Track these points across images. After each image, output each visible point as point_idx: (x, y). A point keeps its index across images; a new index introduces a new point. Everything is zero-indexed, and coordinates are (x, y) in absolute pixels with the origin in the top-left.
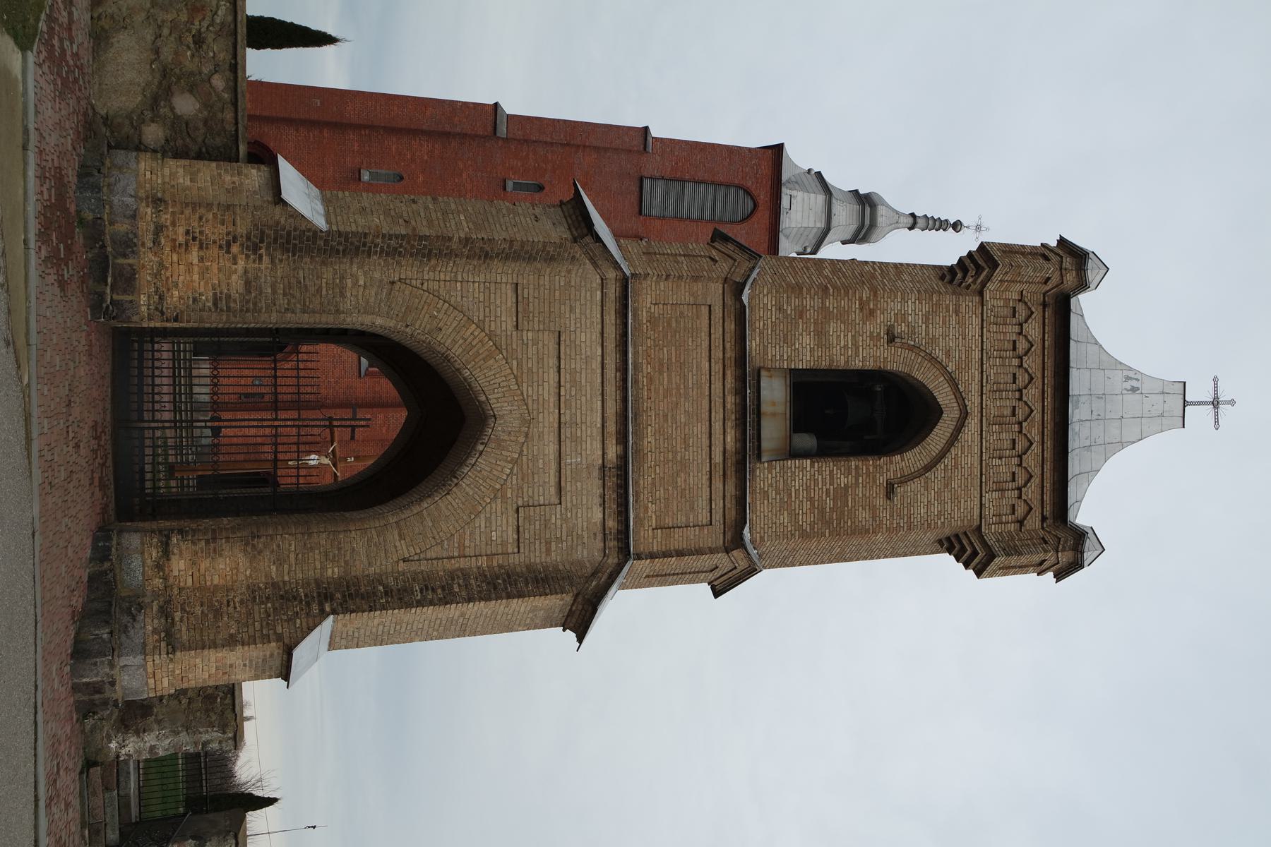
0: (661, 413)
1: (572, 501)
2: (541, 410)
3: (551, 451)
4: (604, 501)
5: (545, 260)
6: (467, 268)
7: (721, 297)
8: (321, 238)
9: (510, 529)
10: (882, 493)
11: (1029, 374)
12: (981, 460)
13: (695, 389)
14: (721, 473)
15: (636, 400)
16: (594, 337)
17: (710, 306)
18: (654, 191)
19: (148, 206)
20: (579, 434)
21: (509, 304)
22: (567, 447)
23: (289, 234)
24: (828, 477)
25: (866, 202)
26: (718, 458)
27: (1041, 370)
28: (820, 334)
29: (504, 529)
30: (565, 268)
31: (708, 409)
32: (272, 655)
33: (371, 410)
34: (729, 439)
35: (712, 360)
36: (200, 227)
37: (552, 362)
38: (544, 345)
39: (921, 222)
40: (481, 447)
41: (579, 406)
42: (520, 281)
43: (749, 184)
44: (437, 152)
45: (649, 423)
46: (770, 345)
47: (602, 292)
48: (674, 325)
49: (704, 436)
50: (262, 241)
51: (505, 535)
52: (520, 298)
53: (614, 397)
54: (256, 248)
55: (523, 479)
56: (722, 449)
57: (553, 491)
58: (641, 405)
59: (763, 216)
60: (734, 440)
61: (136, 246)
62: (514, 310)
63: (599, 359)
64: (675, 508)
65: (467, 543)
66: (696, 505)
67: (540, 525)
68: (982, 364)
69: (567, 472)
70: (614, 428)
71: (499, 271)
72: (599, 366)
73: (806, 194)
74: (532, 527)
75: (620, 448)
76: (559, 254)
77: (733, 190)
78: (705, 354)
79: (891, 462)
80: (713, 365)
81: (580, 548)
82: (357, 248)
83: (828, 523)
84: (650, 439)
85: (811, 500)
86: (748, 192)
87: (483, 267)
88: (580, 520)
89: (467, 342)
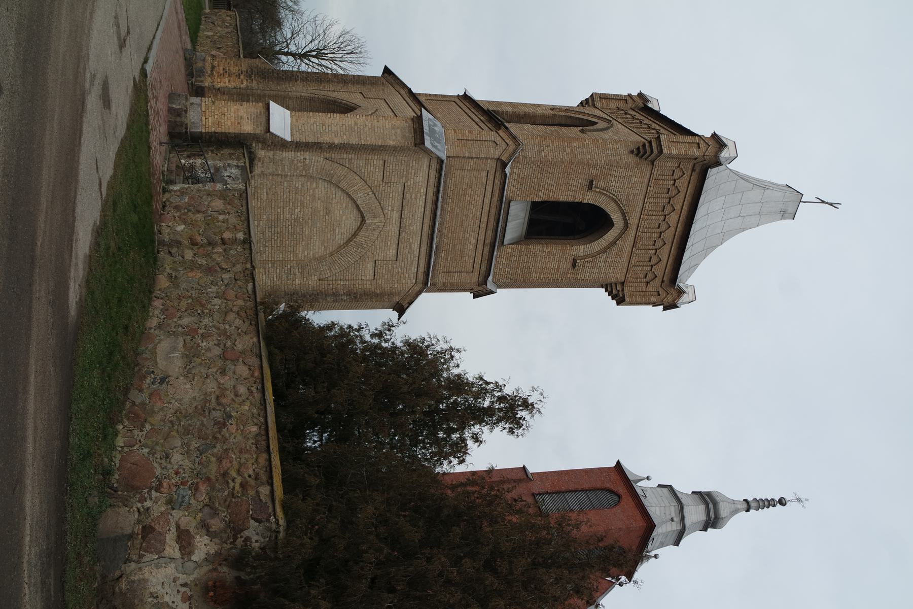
8: (275, 72)
19: (209, 57)
23: (262, 70)
25: (707, 499)
32: (261, 112)
36: (228, 67)
39: (753, 505)
43: (608, 485)
50: (252, 74)
54: (250, 77)
59: (627, 501)
61: (204, 72)
76: (376, 82)
77: (599, 492)
82: (291, 77)
86: (610, 491)
87: (345, 87)
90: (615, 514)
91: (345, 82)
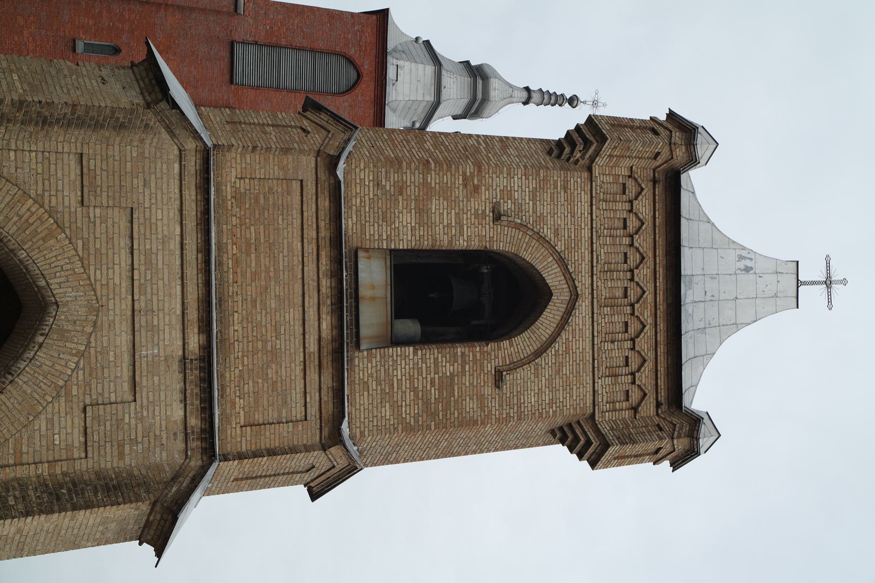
0: (249, 298)
1: (148, 398)
2: (111, 296)
3: (124, 343)
4: (185, 397)
5: (114, 128)
6: (21, 136)
7: (314, 171)
9: (76, 431)
10: (491, 381)
11: (640, 254)
12: (593, 345)
13: (286, 272)
14: (317, 363)
15: (221, 282)
16: (172, 214)
17: (302, 181)
18: (246, 57)
20: (156, 323)
21: (73, 177)
22: (142, 337)
24: (432, 365)
26: (312, 347)
27: (652, 249)
28: (422, 212)
29: (69, 431)
30: (137, 137)
31: (300, 293)
34: (324, 326)
35: (305, 240)
37: (124, 242)
38: (114, 223)
39: (536, 97)
40: (40, 339)
41: (155, 291)
42: (85, 151)
45: (236, 309)
46: (367, 224)
47: (180, 165)
48: (262, 201)
49: (297, 323)
51: (70, 439)
52: (85, 170)
53: (195, 281)
55: (90, 375)
56: (317, 337)
57: (126, 386)
58: (226, 290)
59: (367, 88)
60: (330, 327)
62: (78, 183)
63: (178, 238)
64: (266, 403)
65: (25, 449)
66: (289, 400)
67: (111, 426)
68: (592, 243)
69: (142, 365)
70: (196, 316)
71: (61, 139)
72: (178, 246)
73: (413, 64)
74: (102, 428)
75: (203, 338)
77: (334, 58)
78: (297, 233)
79: (499, 348)
80: (306, 245)
81: (158, 450)
83: (433, 415)
84: (236, 328)
85: (415, 390)
86: (350, 61)
87: (41, 134)
88: (157, 419)
89: (23, 219)
91: (44, 122)
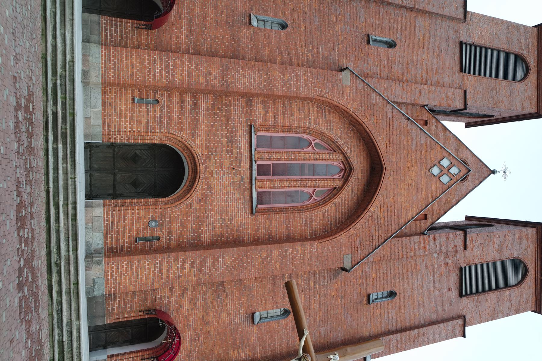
33: (265, 246)
43: (525, 53)
44: (314, 6)
90: (518, 91)
